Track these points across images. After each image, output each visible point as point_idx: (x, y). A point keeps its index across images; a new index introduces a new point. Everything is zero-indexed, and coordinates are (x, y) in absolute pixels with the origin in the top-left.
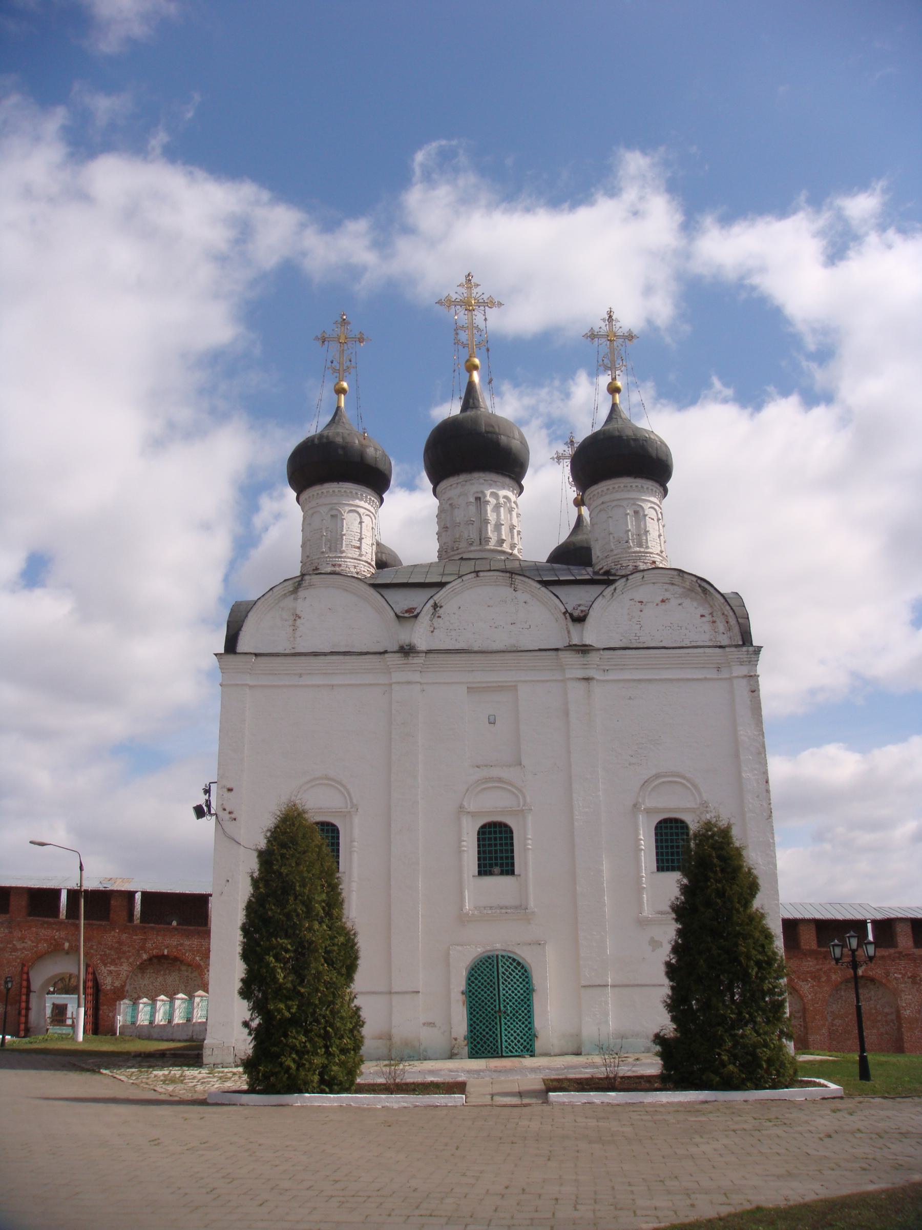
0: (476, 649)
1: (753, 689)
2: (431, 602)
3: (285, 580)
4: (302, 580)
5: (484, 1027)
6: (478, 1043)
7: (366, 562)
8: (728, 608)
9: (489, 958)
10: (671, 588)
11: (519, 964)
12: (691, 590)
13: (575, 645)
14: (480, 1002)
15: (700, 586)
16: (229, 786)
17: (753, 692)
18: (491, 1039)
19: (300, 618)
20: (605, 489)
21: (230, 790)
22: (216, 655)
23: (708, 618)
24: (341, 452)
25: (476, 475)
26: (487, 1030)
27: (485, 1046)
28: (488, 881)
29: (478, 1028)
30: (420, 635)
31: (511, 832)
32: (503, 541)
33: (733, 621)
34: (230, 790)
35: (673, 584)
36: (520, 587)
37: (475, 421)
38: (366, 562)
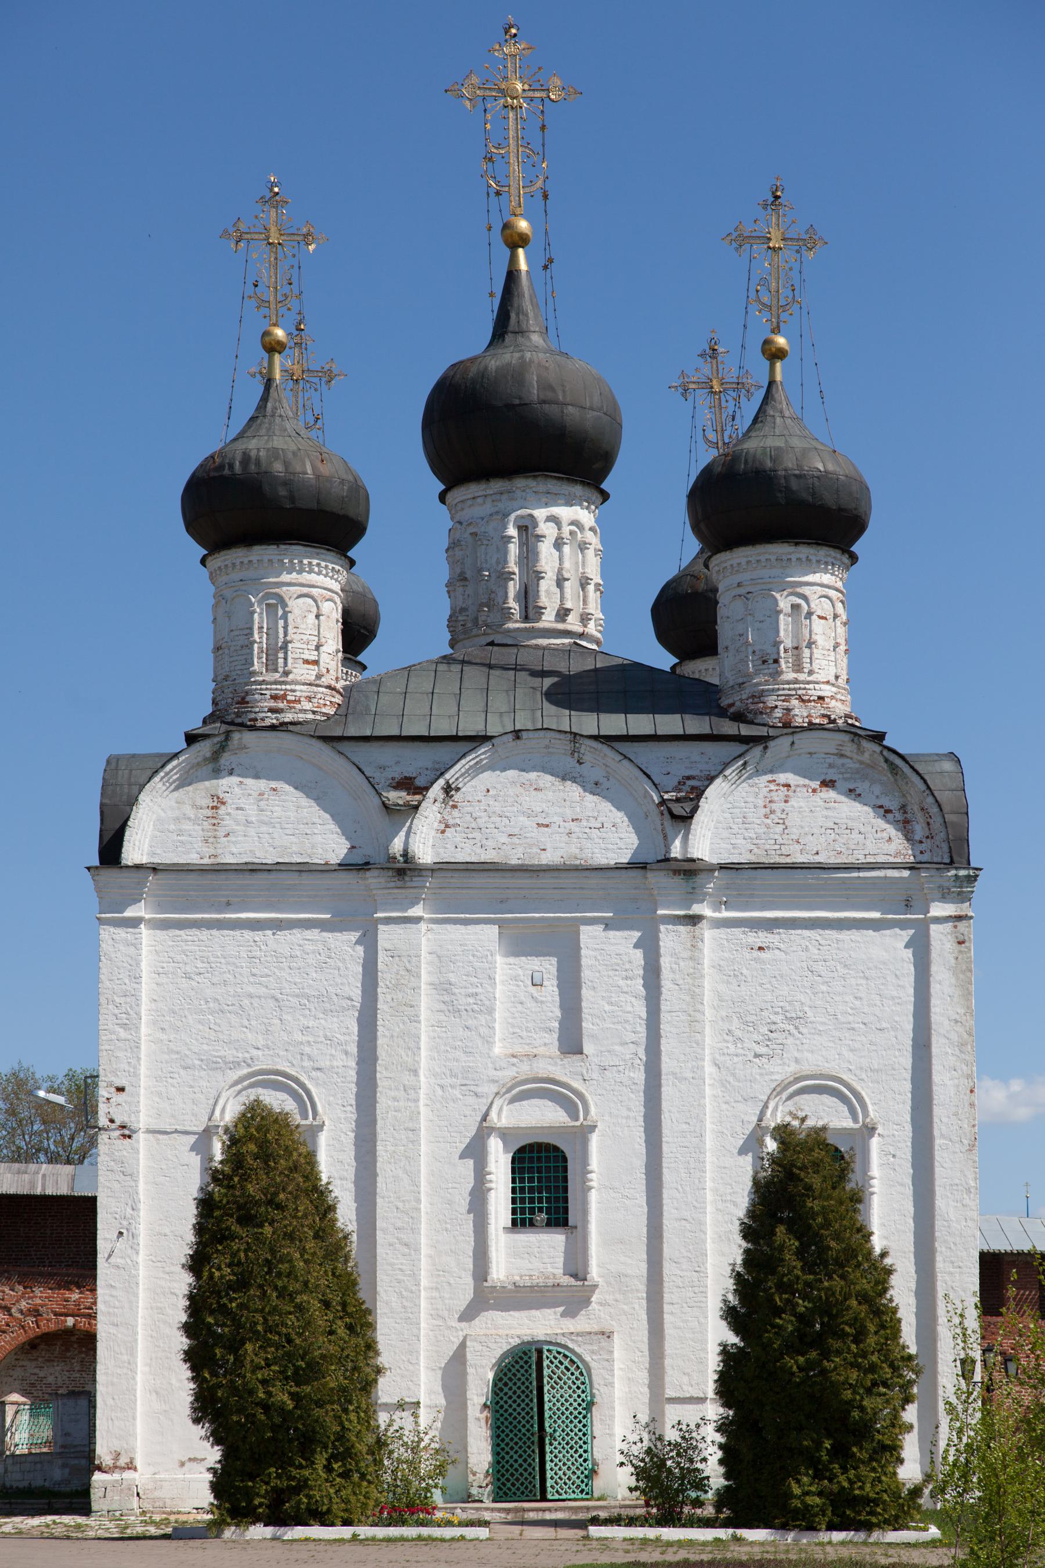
1: (961, 938)
2: (441, 782)
4: (227, 739)
5: (515, 1457)
6: (508, 1480)
7: (329, 687)
8: (930, 799)
9: (525, 1353)
10: (840, 761)
11: (572, 1362)
12: (872, 766)
13: (676, 859)
14: (510, 1419)
16: (120, 1085)
17: (960, 943)
18: (526, 1475)
19: (224, 803)
20: (743, 561)
21: (120, 1090)
22: (89, 868)
23: (899, 816)
24: (282, 492)
25: (520, 482)
26: (520, 1461)
27: (518, 1485)
28: (528, 1238)
29: (507, 1457)
30: (425, 838)
31: (565, 1159)
32: (567, 611)
33: (937, 822)
34: (120, 1090)
35: (842, 755)
36: (587, 758)
37: (518, 374)
38: (329, 687)
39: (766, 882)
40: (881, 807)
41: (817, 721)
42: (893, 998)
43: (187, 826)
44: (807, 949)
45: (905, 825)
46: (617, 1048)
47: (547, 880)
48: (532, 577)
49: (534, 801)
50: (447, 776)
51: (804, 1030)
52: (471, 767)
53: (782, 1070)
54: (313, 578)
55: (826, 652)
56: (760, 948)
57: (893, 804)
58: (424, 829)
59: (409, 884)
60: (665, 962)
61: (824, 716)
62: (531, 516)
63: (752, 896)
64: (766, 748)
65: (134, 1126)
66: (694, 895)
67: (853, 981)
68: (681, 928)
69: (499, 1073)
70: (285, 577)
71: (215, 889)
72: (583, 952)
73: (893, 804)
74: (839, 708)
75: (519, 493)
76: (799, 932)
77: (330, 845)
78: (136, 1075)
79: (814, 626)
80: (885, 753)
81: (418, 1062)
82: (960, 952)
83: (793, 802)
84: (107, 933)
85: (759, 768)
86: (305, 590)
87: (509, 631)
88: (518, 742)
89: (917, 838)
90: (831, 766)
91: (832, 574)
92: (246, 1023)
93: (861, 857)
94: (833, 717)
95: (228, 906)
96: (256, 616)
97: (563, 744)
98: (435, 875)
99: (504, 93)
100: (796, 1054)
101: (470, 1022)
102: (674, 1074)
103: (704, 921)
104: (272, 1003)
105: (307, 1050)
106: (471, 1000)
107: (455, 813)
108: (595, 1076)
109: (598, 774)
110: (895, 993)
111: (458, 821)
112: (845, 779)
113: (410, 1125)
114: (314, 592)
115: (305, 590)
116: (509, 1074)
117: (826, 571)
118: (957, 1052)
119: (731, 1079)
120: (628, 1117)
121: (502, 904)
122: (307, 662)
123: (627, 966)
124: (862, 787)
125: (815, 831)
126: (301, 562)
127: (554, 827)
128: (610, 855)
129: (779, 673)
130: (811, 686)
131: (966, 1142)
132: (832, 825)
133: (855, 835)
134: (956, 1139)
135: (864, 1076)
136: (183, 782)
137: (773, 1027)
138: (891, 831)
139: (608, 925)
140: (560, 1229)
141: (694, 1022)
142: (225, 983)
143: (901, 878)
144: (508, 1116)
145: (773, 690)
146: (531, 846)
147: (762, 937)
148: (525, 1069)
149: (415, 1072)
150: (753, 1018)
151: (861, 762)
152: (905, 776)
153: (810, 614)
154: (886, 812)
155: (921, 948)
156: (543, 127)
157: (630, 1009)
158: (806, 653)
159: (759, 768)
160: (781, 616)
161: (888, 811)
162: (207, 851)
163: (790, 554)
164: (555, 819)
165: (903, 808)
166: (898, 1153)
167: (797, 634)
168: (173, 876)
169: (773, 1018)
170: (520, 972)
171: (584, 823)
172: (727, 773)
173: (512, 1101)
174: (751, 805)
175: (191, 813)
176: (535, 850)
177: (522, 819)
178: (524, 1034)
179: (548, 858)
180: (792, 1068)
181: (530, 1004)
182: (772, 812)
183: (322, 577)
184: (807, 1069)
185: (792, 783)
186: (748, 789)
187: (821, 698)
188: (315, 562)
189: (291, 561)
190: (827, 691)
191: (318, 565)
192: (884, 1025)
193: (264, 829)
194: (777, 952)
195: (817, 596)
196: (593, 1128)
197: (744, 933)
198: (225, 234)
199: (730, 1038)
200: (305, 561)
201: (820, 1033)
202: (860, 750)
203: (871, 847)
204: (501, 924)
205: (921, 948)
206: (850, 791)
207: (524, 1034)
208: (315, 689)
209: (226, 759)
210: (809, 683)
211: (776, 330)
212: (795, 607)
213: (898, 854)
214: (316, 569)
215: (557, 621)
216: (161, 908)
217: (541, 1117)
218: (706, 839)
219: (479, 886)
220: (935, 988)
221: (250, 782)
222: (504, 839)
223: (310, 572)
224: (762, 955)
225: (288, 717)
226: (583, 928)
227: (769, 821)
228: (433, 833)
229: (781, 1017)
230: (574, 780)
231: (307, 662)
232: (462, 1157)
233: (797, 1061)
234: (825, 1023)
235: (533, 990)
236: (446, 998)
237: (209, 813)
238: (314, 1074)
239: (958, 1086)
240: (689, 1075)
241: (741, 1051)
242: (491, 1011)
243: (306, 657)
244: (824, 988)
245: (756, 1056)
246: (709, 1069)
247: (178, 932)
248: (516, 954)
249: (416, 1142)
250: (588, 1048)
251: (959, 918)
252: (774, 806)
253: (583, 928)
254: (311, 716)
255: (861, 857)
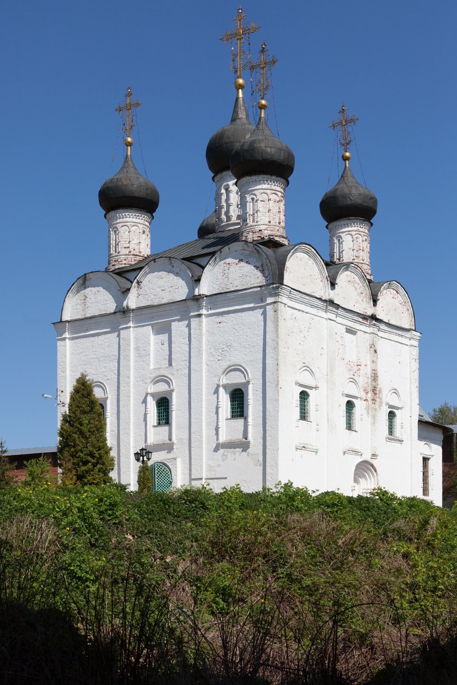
0: (156, 304)
2: (136, 280)
3: (78, 279)
7: (134, 255)
13: (196, 295)
15: (256, 249)
17: (275, 311)
23: (261, 268)
30: (132, 301)
35: (245, 250)
38: (134, 255)
39: (223, 299)
40: (256, 266)
41: (256, 239)
42: (257, 334)
43: (79, 306)
44: (233, 321)
45: (262, 271)
46: (181, 363)
47: (162, 309)
48: (228, 206)
49: (161, 282)
50: (137, 278)
51: (231, 350)
52: (144, 274)
53: (225, 365)
54: (128, 219)
55: (264, 213)
56: (220, 323)
57: (258, 264)
58: (132, 297)
59: (127, 316)
60: (192, 331)
61: (259, 237)
62: (228, 184)
63: (217, 305)
64: (221, 252)
65: (65, 403)
66: (200, 307)
67: (246, 330)
68: (197, 319)
69: (151, 375)
70: (119, 221)
71: (85, 325)
72: (172, 332)
73: (258, 264)
74: (266, 234)
75: (225, 177)
76: (230, 315)
77: (111, 307)
78: (66, 387)
79: (259, 204)
80: (255, 246)
81: (130, 374)
82: (275, 315)
83: (230, 270)
84: (59, 343)
85: (221, 259)
86: (124, 224)
87: (223, 226)
88: (156, 263)
89: (266, 275)
90: (242, 254)
91: (268, 184)
92: (91, 367)
93: (250, 285)
94: (262, 237)
95: (87, 330)
96: (112, 235)
97: (167, 261)
98: (134, 311)
99: (236, 34)
100: (229, 358)
101: (144, 359)
102: (194, 369)
103: (203, 316)
104: (97, 360)
105: (105, 374)
106: (144, 352)
107: (141, 290)
108: (175, 373)
109: (176, 270)
110: (257, 333)
111: (142, 293)
112: (246, 258)
113: (128, 395)
114: (128, 224)
115: (124, 224)
116: (154, 375)
117: (265, 184)
118: (274, 351)
119: (211, 369)
120: (184, 386)
121: (152, 318)
122: (125, 248)
123: (184, 335)
124: (250, 260)
125: (237, 278)
126: (122, 215)
127: (166, 290)
128: (181, 297)
129: (247, 224)
130: (256, 227)
131: (275, 383)
132: (241, 275)
133: (248, 278)
134: (272, 382)
135: (248, 364)
136: (78, 292)
137: (223, 350)
138: (259, 274)
139: (179, 320)
140: (167, 425)
141: (200, 351)
142: (87, 355)
143: (257, 291)
144: (152, 389)
145: (245, 231)
146: (160, 298)
147: (220, 319)
148: (158, 373)
149: (129, 377)
150: (217, 347)
151: (250, 251)
152: (261, 254)
153: (257, 200)
154: (257, 268)
155: (264, 314)
156: (249, 44)
157: (184, 349)
158: (256, 214)
159: (221, 259)
160: (248, 203)
161: (258, 267)
162: (83, 313)
163: (249, 180)
164: (166, 287)
165: (262, 265)
166: (258, 390)
167: (253, 209)
168: (73, 323)
169: (223, 347)
170: (158, 341)
171: (174, 287)
172: (210, 262)
173: (154, 384)
174: (219, 273)
175: (79, 302)
176: (161, 299)
177: (158, 289)
178: (159, 361)
179: (164, 301)
180: (228, 364)
181: (161, 351)
182: (225, 274)
183: (131, 219)
184: (232, 363)
185: (230, 263)
186: (218, 267)
187: (260, 230)
188: (127, 214)
189: (122, 215)
190: (262, 227)
191: (132, 215)
192: (255, 344)
193: (96, 304)
194: (224, 323)
195: (260, 193)
196: (173, 390)
197: (215, 318)
198: (116, 110)
199: (211, 355)
200: (123, 214)
201: (236, 350)
202: (249, 247)
203: (253, 282)
204: (152, 325)
205: (264, 314)
206: (247, 262)
207: (159, 361)
208: (128, 256)
209: (87, 283)
210: (256, 226)
211: (263, 98)
212: (253, 199)
213: (261, 282)
214: (128, 216)
215: (237, 220)
216: (72, 333)
217: (162, 387)
218: (204, 288)
219: (147, 313)
220: (268, 329)
221: (93, 289)
222: (153, 297)
223: (126, 217)
224: (220, 325)
225: (117, 267)
226: (172, 323)
227: (223, 277)
228: (135, 298)
229: (225, 346)
230: (171, 273)
231: (125, 248)
232: (142, 403)
233: (229, 361)
234: (237, 346)
235: (161, 346)
236: (138, 352)
237: (83, 301)
238: (107, 381)
239: (273, 363)
240: (198, 369)
241: (214, 359)
242: (149, 355)
243: (125, 246)
244: (237, 334)
245: (218, 360)
246: (204, 367)
247: (76, 340)
248: (155, 335)
249: (129, 400)
250: (173, 364)
251: (275, 302)
252: (225, 272)
253: (172, 323)
254: (124, 265)
255: (250, 285)
